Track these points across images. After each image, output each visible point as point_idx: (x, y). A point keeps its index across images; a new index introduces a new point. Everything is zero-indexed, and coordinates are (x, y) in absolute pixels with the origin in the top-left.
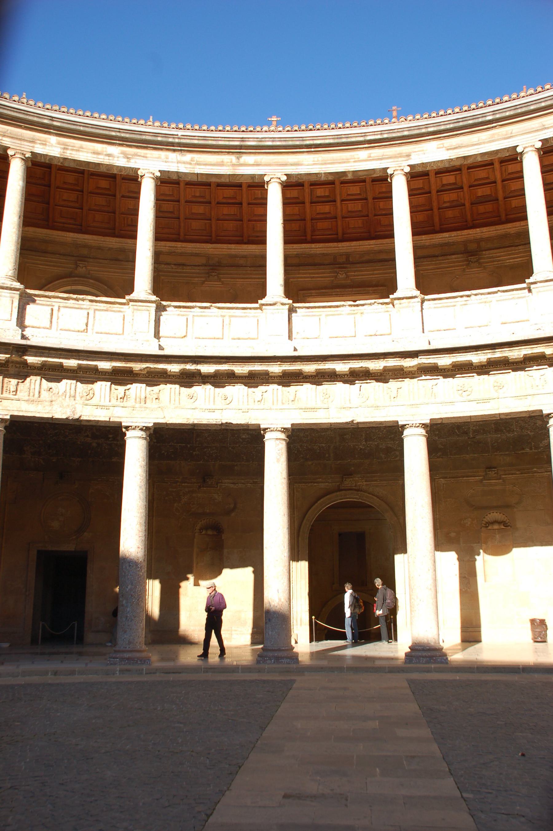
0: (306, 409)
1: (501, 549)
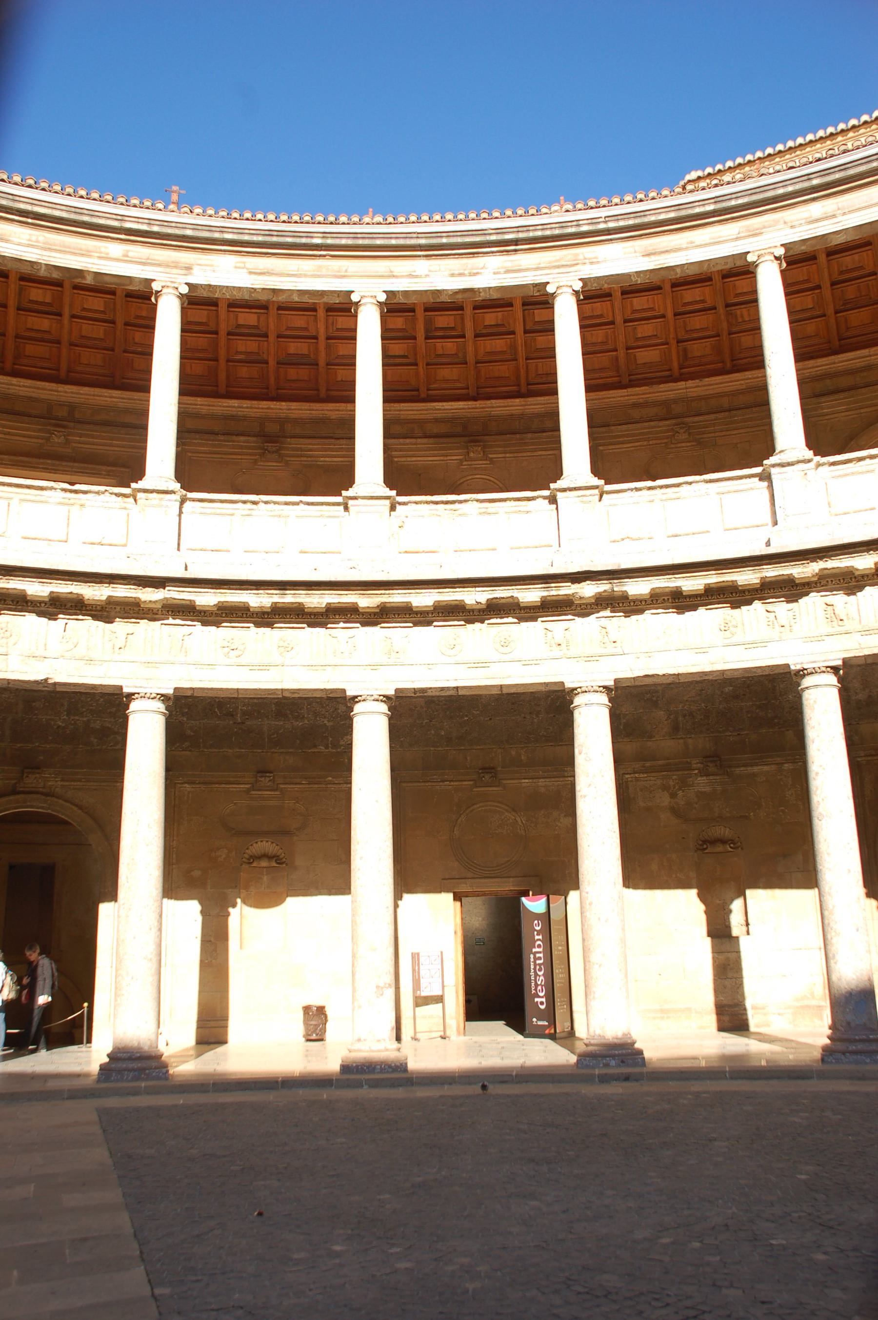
1: (267, 898)
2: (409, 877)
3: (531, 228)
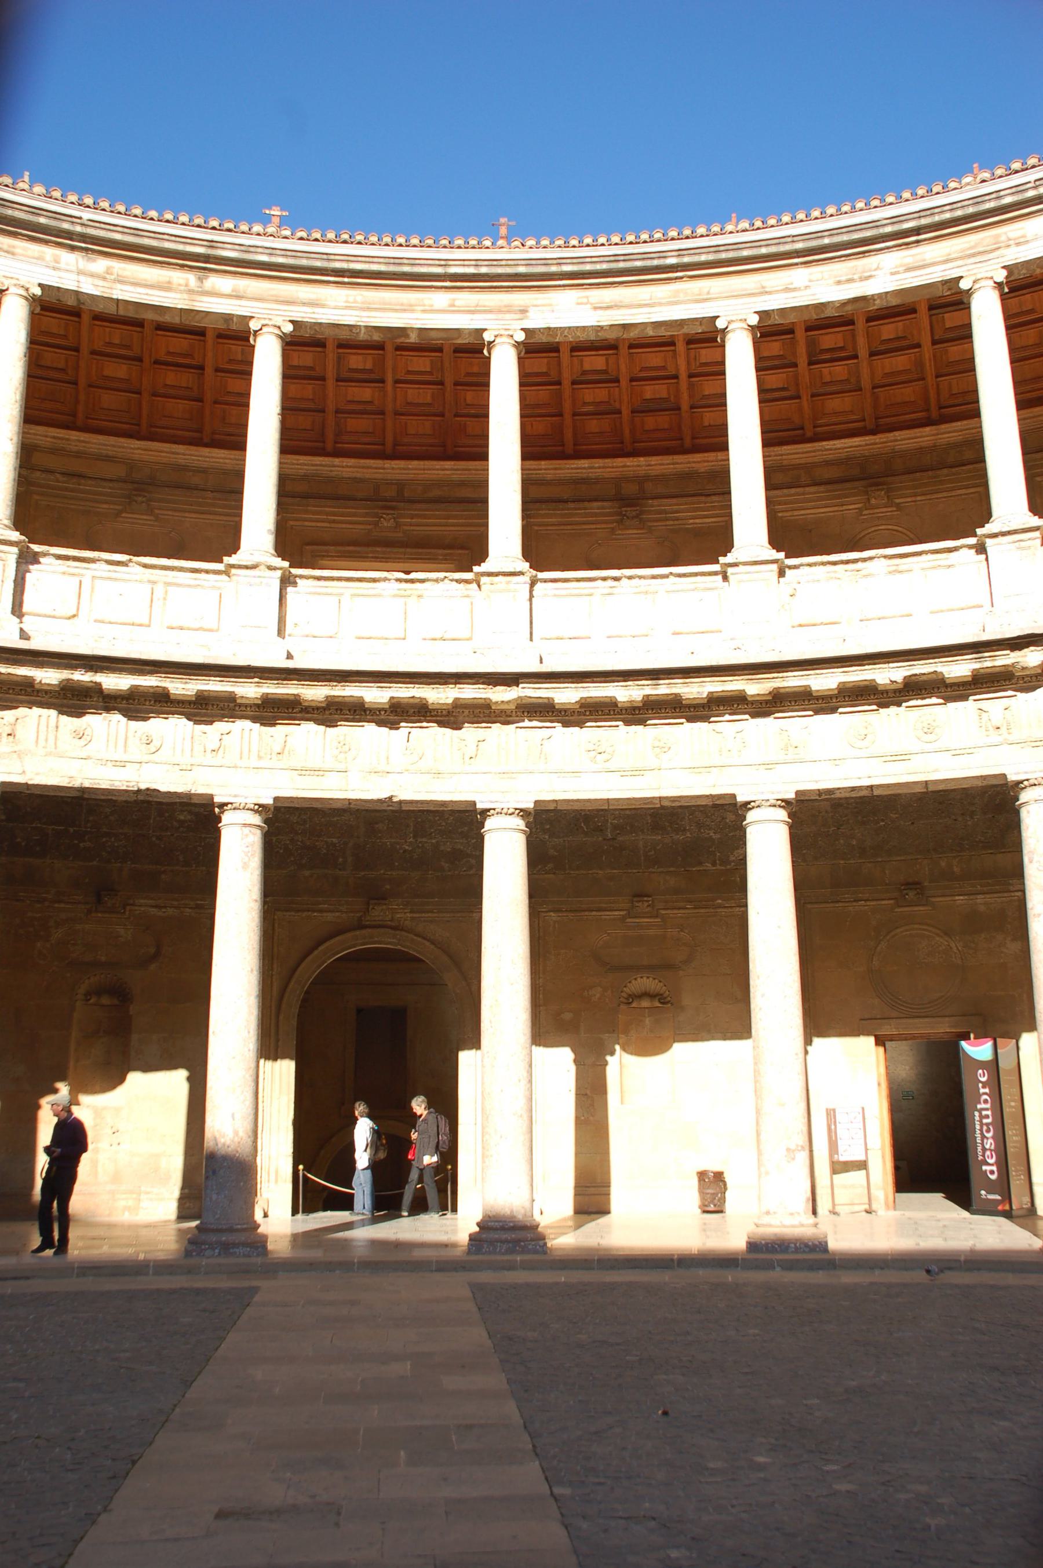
0: (303, 771)
1: (651, 1045)
2: (820, 1018)
3: (936, 210)
